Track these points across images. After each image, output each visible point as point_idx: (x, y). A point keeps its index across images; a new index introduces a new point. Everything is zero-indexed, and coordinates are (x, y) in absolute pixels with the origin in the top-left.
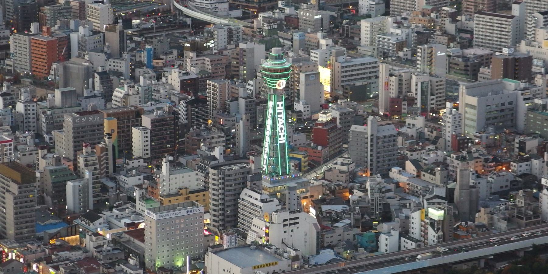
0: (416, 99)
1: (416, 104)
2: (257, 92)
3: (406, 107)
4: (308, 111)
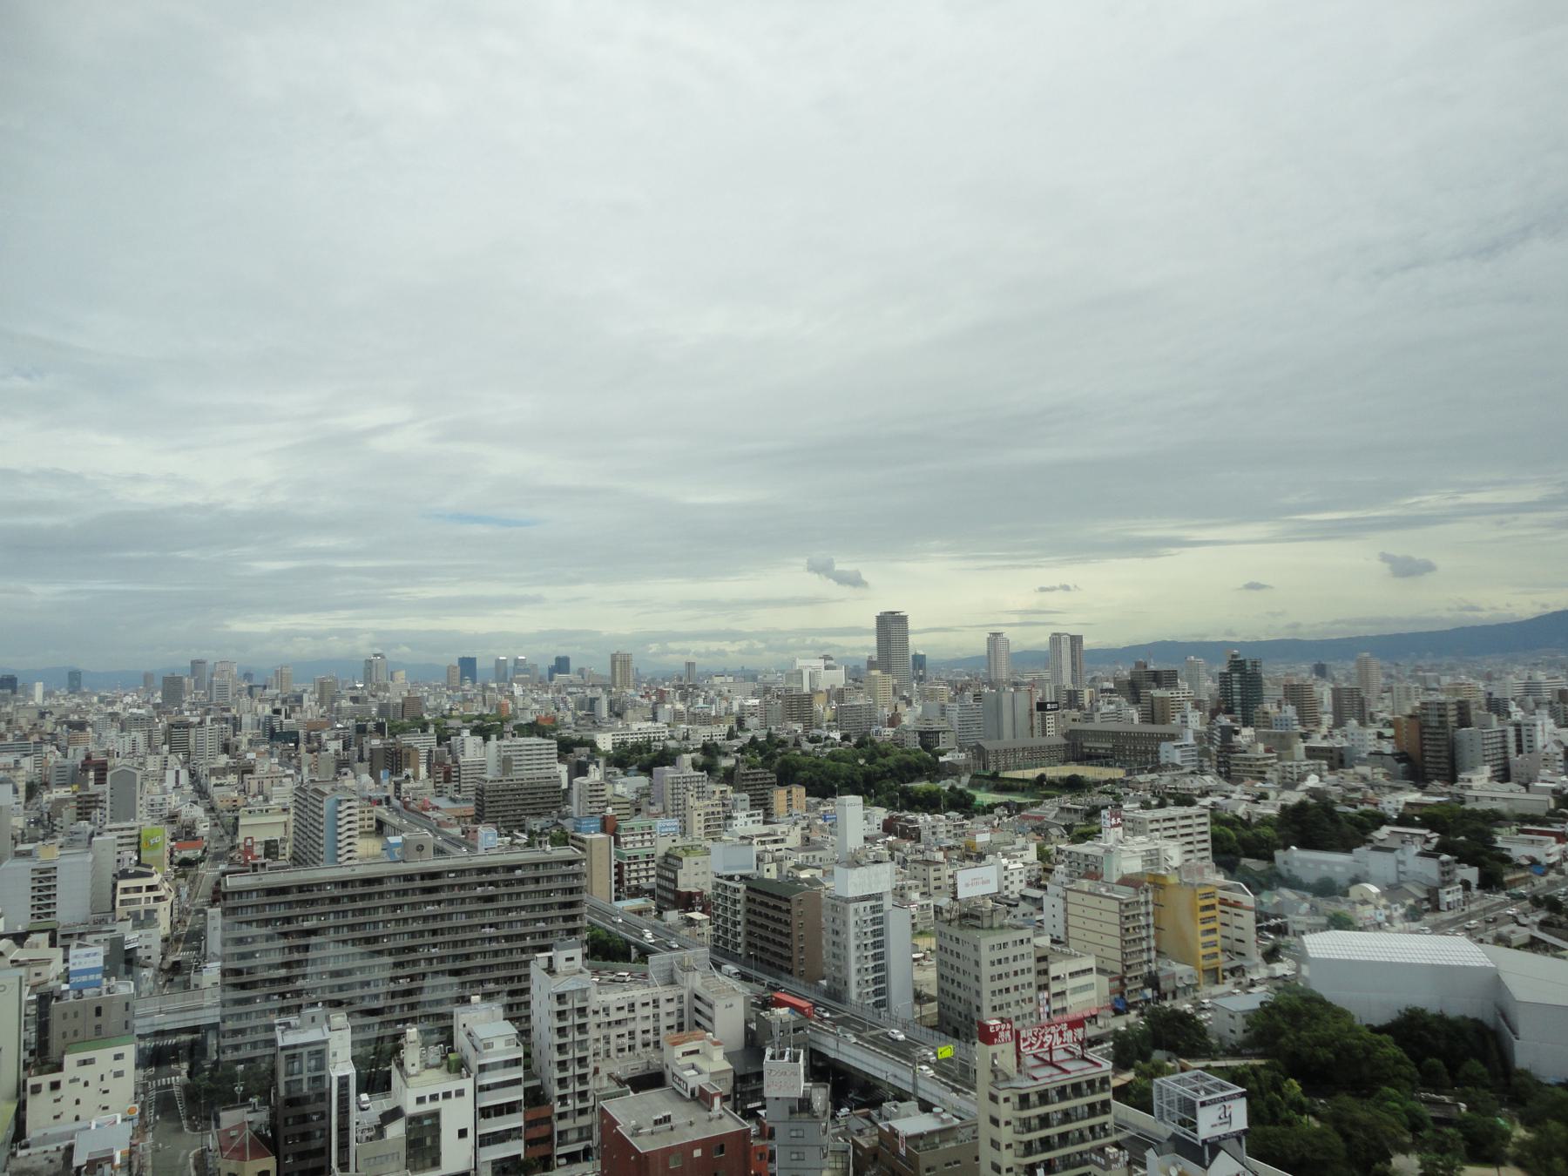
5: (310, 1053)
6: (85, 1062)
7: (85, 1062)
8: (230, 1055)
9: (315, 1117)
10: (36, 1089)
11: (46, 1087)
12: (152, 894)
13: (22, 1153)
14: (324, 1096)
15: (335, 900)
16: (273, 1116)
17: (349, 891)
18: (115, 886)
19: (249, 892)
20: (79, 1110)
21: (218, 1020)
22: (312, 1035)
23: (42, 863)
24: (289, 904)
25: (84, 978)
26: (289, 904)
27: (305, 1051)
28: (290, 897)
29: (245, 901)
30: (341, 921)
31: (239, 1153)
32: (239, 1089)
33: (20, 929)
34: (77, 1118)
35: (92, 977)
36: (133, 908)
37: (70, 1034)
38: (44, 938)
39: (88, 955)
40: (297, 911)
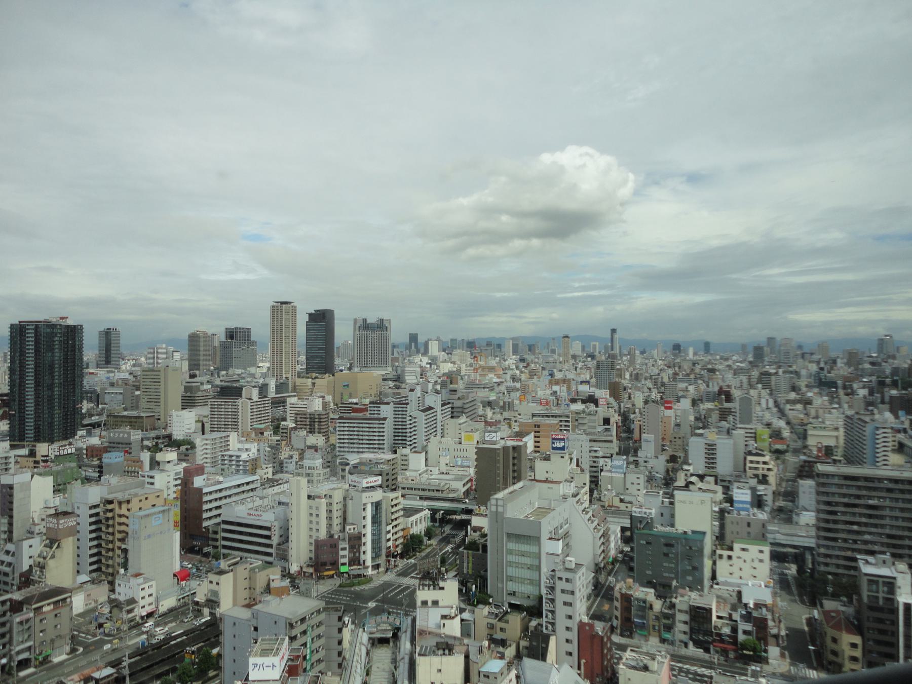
0: (364, 535)
1: (364, 544)
2: (25, 568)
3: (346, 553)
4: (150, 595)
5: (884, 582)
6: (743, 550)
7: (743, 550)
8: (822, 568)
9: (888, 622)
10: (721, 556)
11: (725, 557)
12: (766, 466)
13: (715, 586)
14: (895, 611)
15: (889, 490)
16: (858, 612)
17: (900, 486)
18: (745, 459)
19: (833, 476)
20: (741, 573)
21: (813, 545)
22: (885, 571)
23: (710, 441)
24: (859, 488)
25: (741, 505)
26: (859, 488)
27: (881, 580)
28: (859, 483)
29: (830, 481)
30: (893, 504)
31: (837, 627)
32: (830, 589)
33: (701, 473)
34: (741, 578)
35: (745, 506)
36: (756, 472)
37: (735, 533)
38: (712, 479)
39: (743, 494)
40: (864, 493)
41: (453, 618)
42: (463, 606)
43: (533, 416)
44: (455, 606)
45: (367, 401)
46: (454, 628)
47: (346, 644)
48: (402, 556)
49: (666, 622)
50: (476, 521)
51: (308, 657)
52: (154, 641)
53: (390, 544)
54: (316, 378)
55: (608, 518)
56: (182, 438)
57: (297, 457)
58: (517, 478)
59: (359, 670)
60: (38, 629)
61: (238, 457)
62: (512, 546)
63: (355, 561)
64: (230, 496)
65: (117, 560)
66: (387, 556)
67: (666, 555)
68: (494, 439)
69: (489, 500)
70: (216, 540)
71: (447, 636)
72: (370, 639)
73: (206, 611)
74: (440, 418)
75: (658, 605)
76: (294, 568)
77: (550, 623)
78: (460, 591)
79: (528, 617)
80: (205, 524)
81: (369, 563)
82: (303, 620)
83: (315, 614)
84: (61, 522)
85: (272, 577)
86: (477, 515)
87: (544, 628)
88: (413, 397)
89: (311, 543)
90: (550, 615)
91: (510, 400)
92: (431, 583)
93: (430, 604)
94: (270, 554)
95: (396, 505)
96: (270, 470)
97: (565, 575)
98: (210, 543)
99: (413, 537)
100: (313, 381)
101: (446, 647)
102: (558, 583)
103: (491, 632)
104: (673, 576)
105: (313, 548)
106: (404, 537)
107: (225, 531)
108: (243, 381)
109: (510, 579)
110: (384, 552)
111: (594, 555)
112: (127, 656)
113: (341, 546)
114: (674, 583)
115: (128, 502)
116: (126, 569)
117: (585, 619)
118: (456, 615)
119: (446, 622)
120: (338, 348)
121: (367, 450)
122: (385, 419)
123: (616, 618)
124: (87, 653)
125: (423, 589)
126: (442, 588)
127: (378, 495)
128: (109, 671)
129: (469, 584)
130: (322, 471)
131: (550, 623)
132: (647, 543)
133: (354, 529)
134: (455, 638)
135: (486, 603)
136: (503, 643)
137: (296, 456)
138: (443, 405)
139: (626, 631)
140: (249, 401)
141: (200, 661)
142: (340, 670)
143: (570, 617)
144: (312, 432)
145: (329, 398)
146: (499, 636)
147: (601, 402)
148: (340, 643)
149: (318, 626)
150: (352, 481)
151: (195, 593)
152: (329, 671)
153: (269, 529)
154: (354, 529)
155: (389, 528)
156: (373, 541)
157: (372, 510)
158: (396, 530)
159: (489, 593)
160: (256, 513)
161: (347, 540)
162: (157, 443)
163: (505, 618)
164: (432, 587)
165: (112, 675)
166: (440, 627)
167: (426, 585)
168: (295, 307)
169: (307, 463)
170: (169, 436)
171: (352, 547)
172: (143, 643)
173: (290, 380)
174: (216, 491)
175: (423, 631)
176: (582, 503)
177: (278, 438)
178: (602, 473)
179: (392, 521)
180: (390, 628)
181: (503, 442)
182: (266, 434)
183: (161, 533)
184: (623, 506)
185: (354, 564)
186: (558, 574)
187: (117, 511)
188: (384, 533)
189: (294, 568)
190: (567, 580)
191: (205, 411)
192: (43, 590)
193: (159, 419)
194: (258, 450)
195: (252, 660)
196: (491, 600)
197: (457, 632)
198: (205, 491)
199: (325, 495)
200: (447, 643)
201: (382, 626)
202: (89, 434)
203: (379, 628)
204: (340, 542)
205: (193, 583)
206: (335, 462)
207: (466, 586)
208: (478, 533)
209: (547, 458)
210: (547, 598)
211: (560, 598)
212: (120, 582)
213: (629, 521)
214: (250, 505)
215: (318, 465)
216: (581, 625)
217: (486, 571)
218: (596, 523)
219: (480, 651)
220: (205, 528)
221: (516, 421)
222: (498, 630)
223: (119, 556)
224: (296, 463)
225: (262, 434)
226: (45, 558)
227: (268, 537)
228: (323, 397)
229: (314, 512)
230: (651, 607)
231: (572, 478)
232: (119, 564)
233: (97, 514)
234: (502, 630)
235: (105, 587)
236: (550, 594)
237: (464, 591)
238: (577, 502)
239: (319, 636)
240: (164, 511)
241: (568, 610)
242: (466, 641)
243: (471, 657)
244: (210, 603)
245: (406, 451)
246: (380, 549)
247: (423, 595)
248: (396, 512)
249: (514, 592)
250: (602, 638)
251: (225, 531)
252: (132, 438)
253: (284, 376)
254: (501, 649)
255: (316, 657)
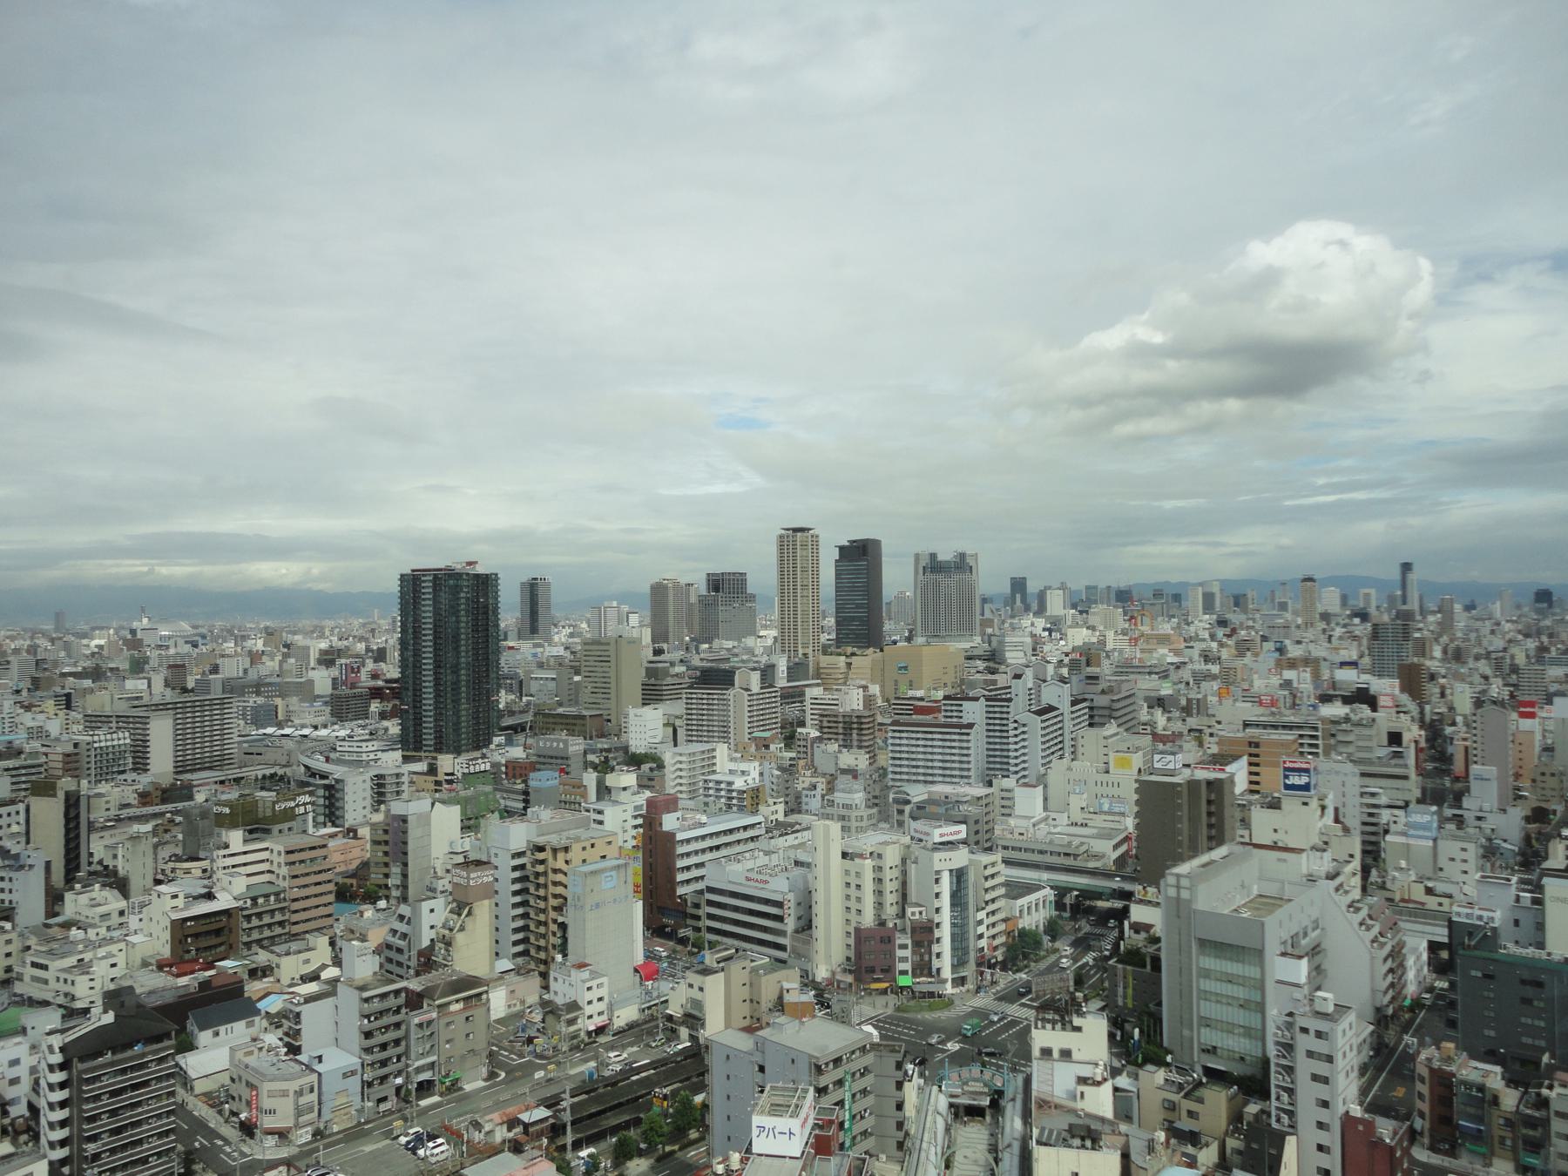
0: (938, 925)
1: (938, 940)
2: (425, 943)
3: (907, 953)
4: (600, 999)
41: (1099, 1084)
42: (1116, 1064)
43: (1246, 725)
44: (1101, 1063)
45: (940, 694)
46: (1100, 1102)
47: (910, 1110)
48: (1004, 966)
49: (1531, 1133)
50: (1138, 913)
51: (847, 1125)
52: (607, 1073)
53: (983, 943)
54: (853, 654)
55: (1401, 924)
56: (643, 752)
57: (824, 786)
58: (1217, 839)
59: (932, 1158)
60: (444, 1035)
61: (730, 783)
62: (1209, 962)
63: (923, 968)
64: (718, 848)
65: (553, 940)
66: (979, 965)
67: (1527, 1001)
68: (1171, 766)
69: (1163, 876)
70: (698, 918)
71: (1088, 1115)
72: (951, 1105)
73: (684, 1032)
74: (1068, 725)
75: (1510, 1099)
76: (822, 974)
77: (1285, 1111)
78: (1111, 1036)
79: (1241, 1096)
80: (680, 891)
81: (947, 973)
82: (837, 1061)
83: (858, 1053)
84: (472, 875)
85: (786, 985)
86: (1141, 902)
87: (1274, 1119)
88: (1020, 689)
89: (848, 933)
90: (1285, 1097)
91: (1200, 696)
92: (1057, 1017)
93: (1056, 1054)
94: (782, 948)
95: (993, 876)
96: (781, 808)
97: (1314, 1024)
98: (689, 922)
99: (1023, 933)
100: (849, 660)
101: (1086, 1135)
102: (1300, 1037)
103: (1170, 1116)
104: (1543, 1043)
105: (851, 941)
106: (1009, 934)
107: (710, 903)
108: (736, 659)
109: (1206, 1022)
110: (972, 956)
111: (1374, 991)
112: (568, 1092)
113: (898, 942)
114: (1546, 1058)
115: (566, 849)
116: (565, 955)
117: (1357, 1111)
118: (1105, 1080)
119: (1086, 1089)
120: (889, 604)
121: (940, 779)
122: (970, 726)
123: (1422, 1115)
124: (516, 1079)
125: (1044, 1027)
126: (1078, 1029)
127: (960, 857)
128: (542, 1113)
129: (1127, 1027)
130: (865, 813)
131: (1285, 1111)
132: (1486, 976)
133: (921, 913)
134: (1103, 1120)
135: (1161, 1063)
136: (1193, 1138)
137: (821, 787)
138: (1074, 703)
139: (1444, 1141)
140: (746, 693)
141: (677, 1111)
142: (900, 1154)
143: (1325, 1104)
144: (847, 745)
145: (875, 689)
146: (1185, 1124)
147: (1383, 701)
148: (900, 1106)
149: (862, 1075)
150: (916, 831)
151: (666, 1001)
152: (883, 1152)
153: (779, 904)
154: (921, 913)
155: (981, 915)
156: (953, 935)
157: (951, 883)
158: (992, 919)
159: (1165, 1044)
160: (760, 877)
161: (909, 931)
162: (606, 758)
163: (1197, 1094)
164: (1059, 1026)
165: (546, 1119)
166: (1075, 1097)
167: (1049, 1021)
168: (817, 536)
169: (839, 797)
170: (626, 749)
171: (917, 944)
172: (591, 1075)
173: (811, 658)
174: (696, 839)
175: (1044, 1101)
176: (1346, 892)
177: (793, 755)
178: (1388, 838)
179: (987, 903)
180: (986, 1090)
181: (1187, 772)
182: (772, 747)
183: (615, 900)
184: (1432, 902)
185: (922, 975)
186: (1301, 1022)
187: (551, 863)
188: (971, 923)
189: (822, 974)
190: (1319, 1035)
191: (678, 708)
192: (449, 979)
193: (609, 721)
194: (761, 774)
195: (757, 1120)
196: (1169, 1058)
197: (1108, 1113)
198: (679, 837)
199: (871, 853)
200: (1089, 1129)
201: (972, 1084)
202: (510, 742)
203: (966, 1088)
204: (898, 935)
205: (664, 986)
206: (886, 797)
207: (1122, 1029)
208: (1143, 935)
209: (1275, 805)
210: (1278, 1065)
211: (1305, 1067)
212: (557, 975)
213: (1445, 931)
214: (750, 864)
215: (857, 802)
216: (1347, 1120)
217: (1160, 1004)
218: (1376, 930)
219: (1151, 1148)
220: (680, 897)
221: (1211, 735)
222: (1184, 1114)
223: (554, 934)
224: (823, 796)
225: (767, 747)
226: (451, 930)
227: (780, 919)
228: (865, 688)
229: (854, 881)
230: (1495, 1101)
231: (1326, 843)
232: (554, 946)
233: (522, 867)
234: (1191, 1114)
235: (536, 981)
236: (1284, 1057)
237: (1118, 1038)
238: (1337, 890)
239: (864, 1092)
240: (618, 867)
241: (1321, 1091)
242: (1123, 1127)
243: (1134, 1157)
244: (690, 1020)
245: (1009, 783)
246: (966, 951)
247: (1043, 1037)
248: (993, 888)
249: (1215, 1048)
250: (1392, 1150)
251: (710, 903)
252: (571, 749)
253: (801, 651)
254: (1190, 1149)
255: (859, 1127)
